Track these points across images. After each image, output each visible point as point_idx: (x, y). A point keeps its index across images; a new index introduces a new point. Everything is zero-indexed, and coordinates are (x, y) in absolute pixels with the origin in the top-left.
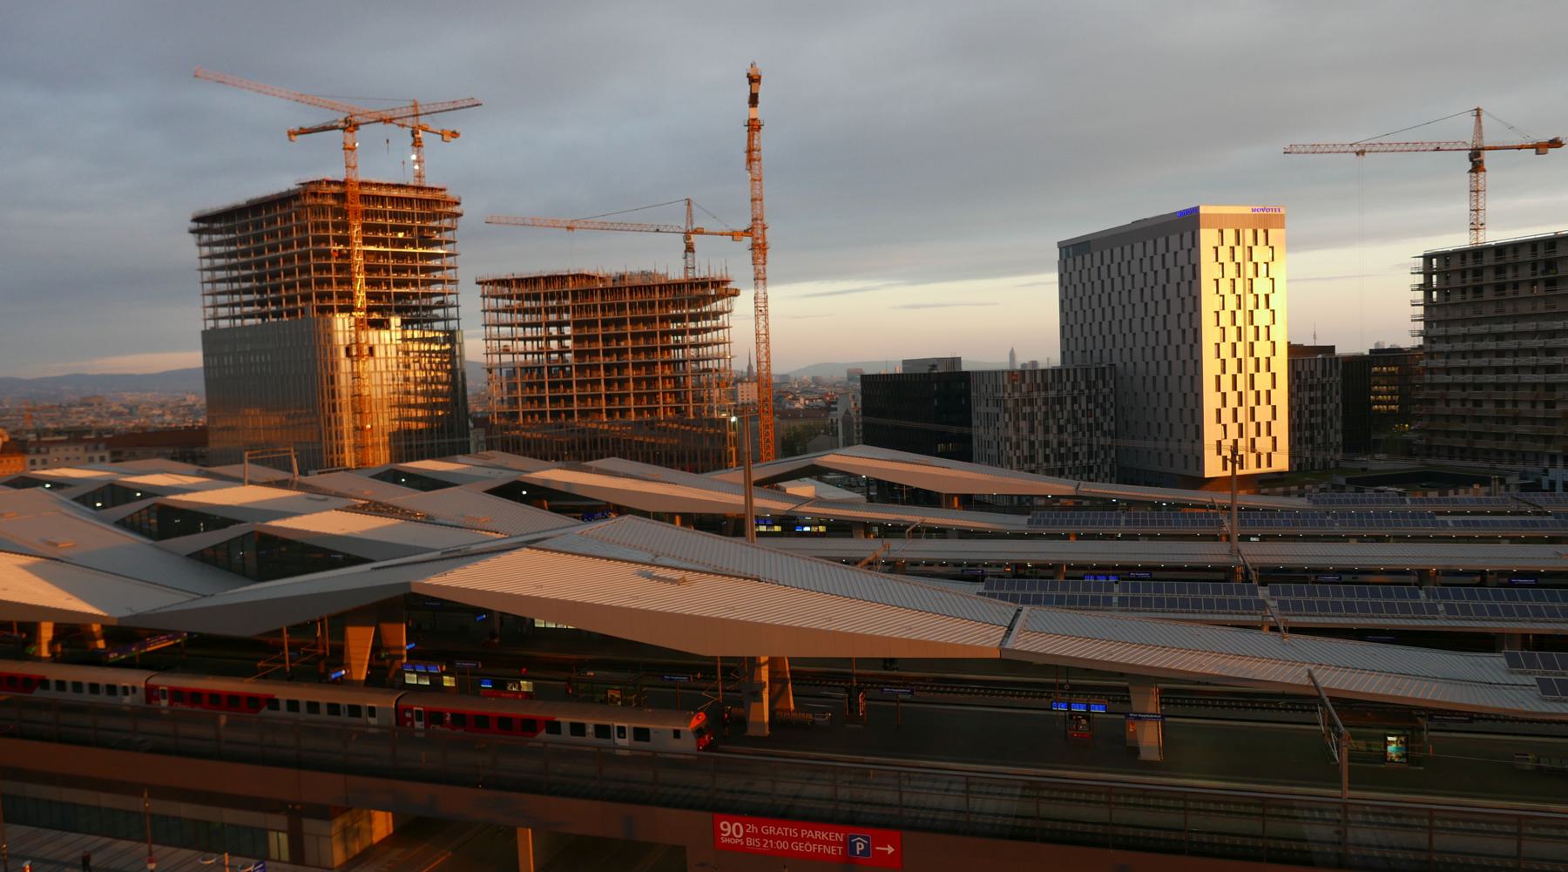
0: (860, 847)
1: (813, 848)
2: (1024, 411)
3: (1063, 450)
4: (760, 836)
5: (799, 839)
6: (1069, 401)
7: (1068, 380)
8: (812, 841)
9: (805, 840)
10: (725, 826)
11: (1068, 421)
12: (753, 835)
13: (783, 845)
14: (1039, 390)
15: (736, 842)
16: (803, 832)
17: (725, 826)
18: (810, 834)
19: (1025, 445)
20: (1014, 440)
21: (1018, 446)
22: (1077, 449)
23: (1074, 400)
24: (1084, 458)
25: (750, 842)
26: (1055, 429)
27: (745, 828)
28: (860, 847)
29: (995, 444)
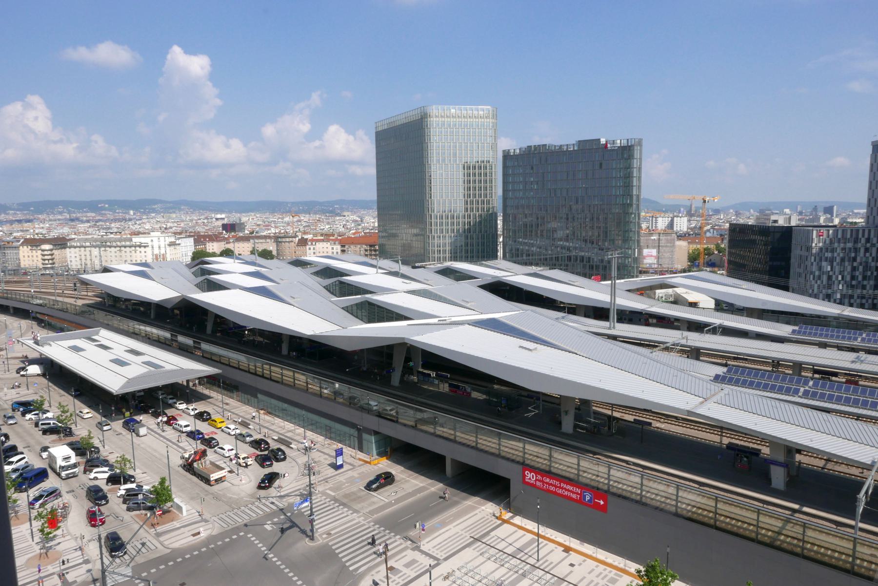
0: (588, 498)
1: (566, 493)
2: (826, 255)
3: (854, 283)
4: (542, 481)
5: (560, 487)
6: (862, 250)
7: (863, 236)
8: (566, 490)
9: (562, 488)
10: (528, 474)
11: (861, 264)
12: (539, 481)
13: (552, 488)
14: (839, 242)
15: (532, 482)
16: (562, 485)
17: (528, 474)
18: (565, 486)
19: (825, 278)
20: (817, 273)
21: (819, 277)
22: (865, 283)
23: (867, 250)
24: (871, 289)
25: (538, 484)
26: (849, 269)
27: (536, 476)
28: (588, 498)
29: (804, 275)
